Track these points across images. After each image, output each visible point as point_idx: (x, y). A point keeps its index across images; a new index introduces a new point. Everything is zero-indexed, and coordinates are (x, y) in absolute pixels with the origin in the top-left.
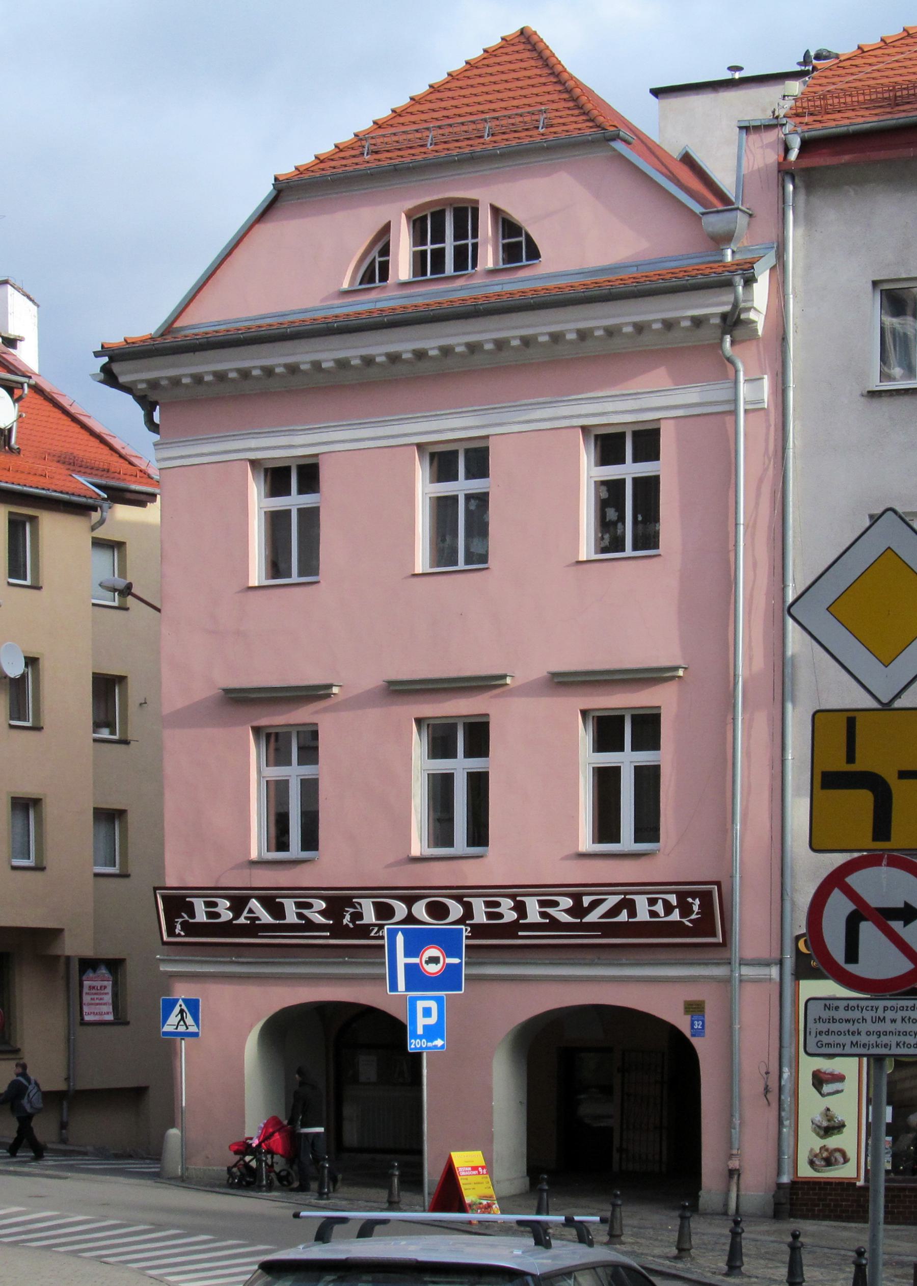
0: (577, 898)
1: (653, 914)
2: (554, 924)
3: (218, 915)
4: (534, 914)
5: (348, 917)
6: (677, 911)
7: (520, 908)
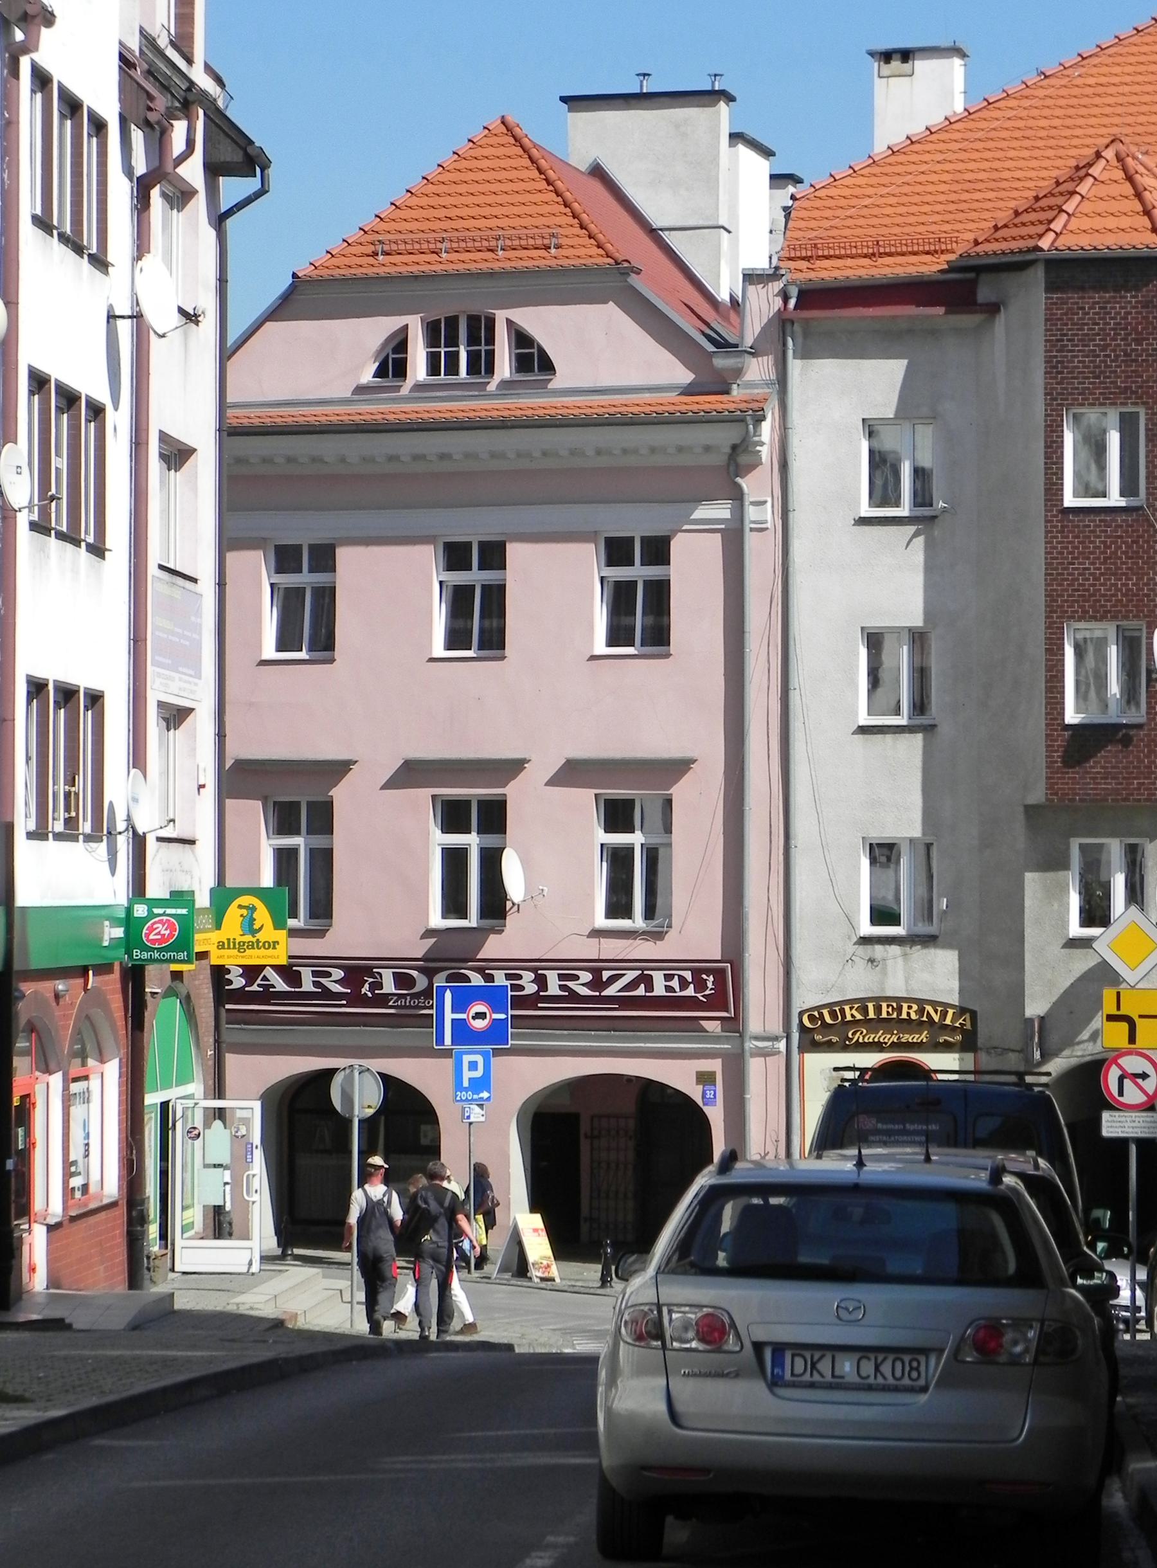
0: (597, 972)
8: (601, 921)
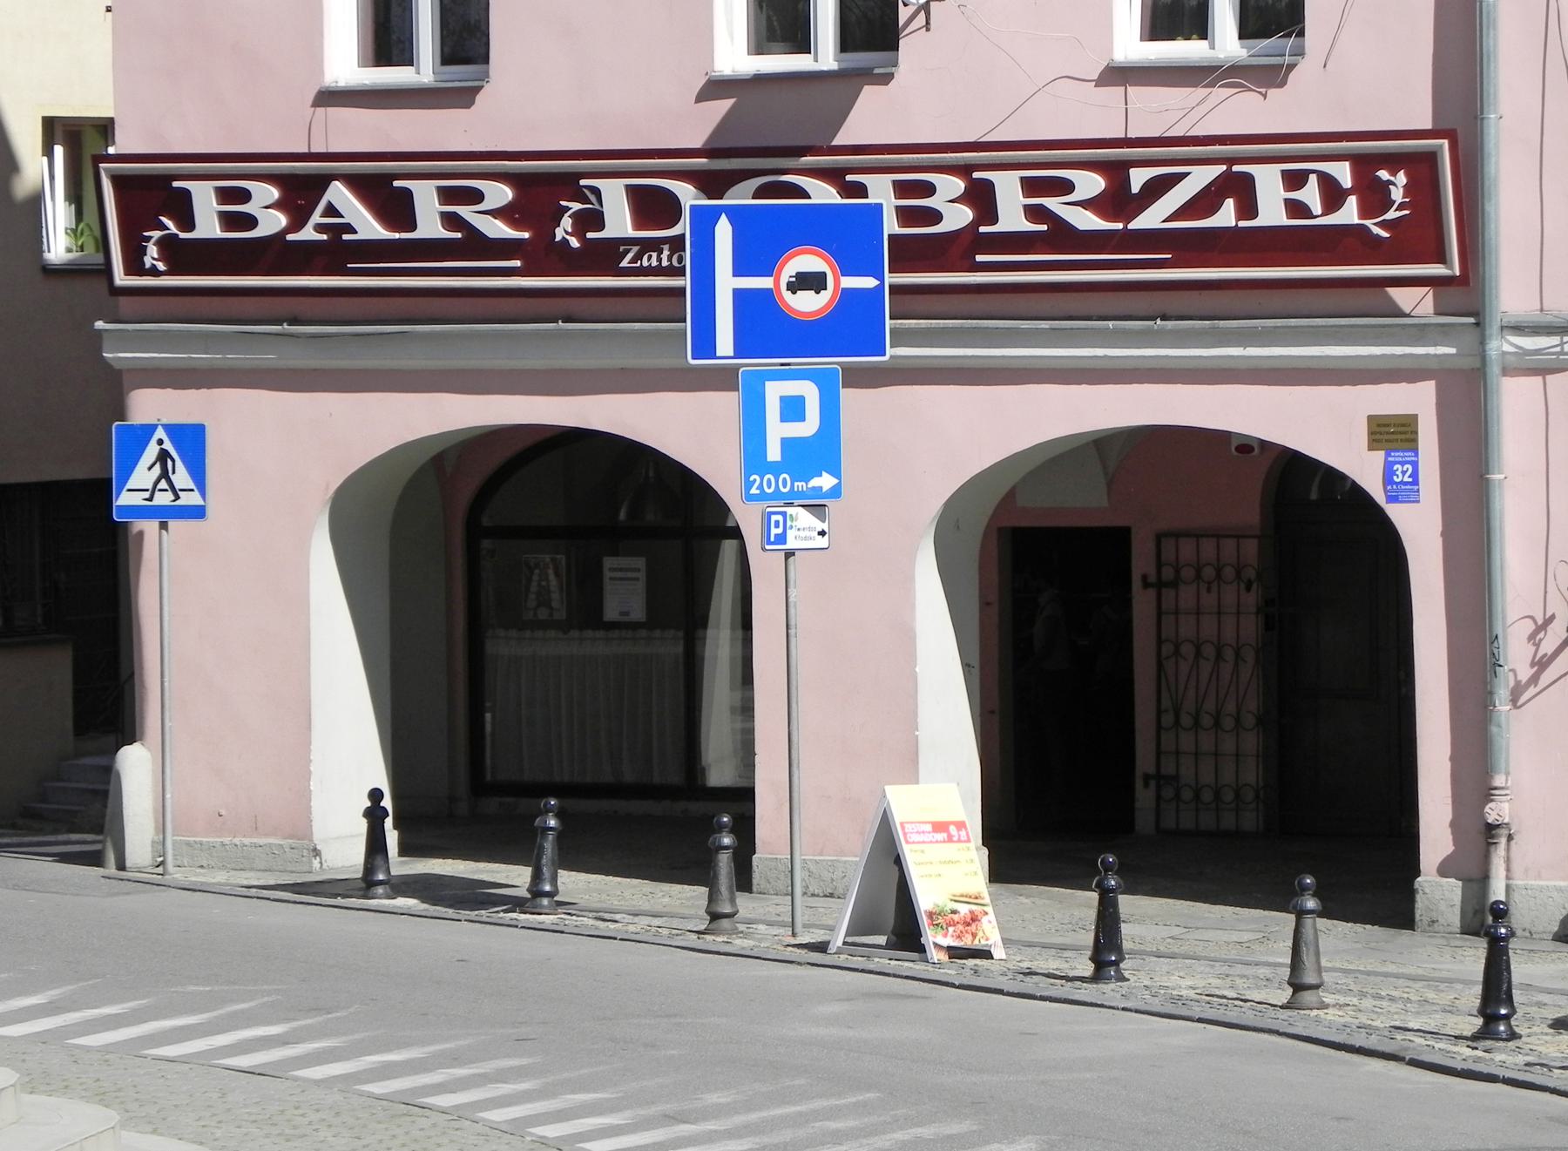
0: (1116, 172)
1: (1296, 208)
2: (1061, 236)
3: (250, 222)
4: (1012, 216)
5: (567, 222)
6: (1352, 201)
7: (982, 198)
8: (1129, 43)
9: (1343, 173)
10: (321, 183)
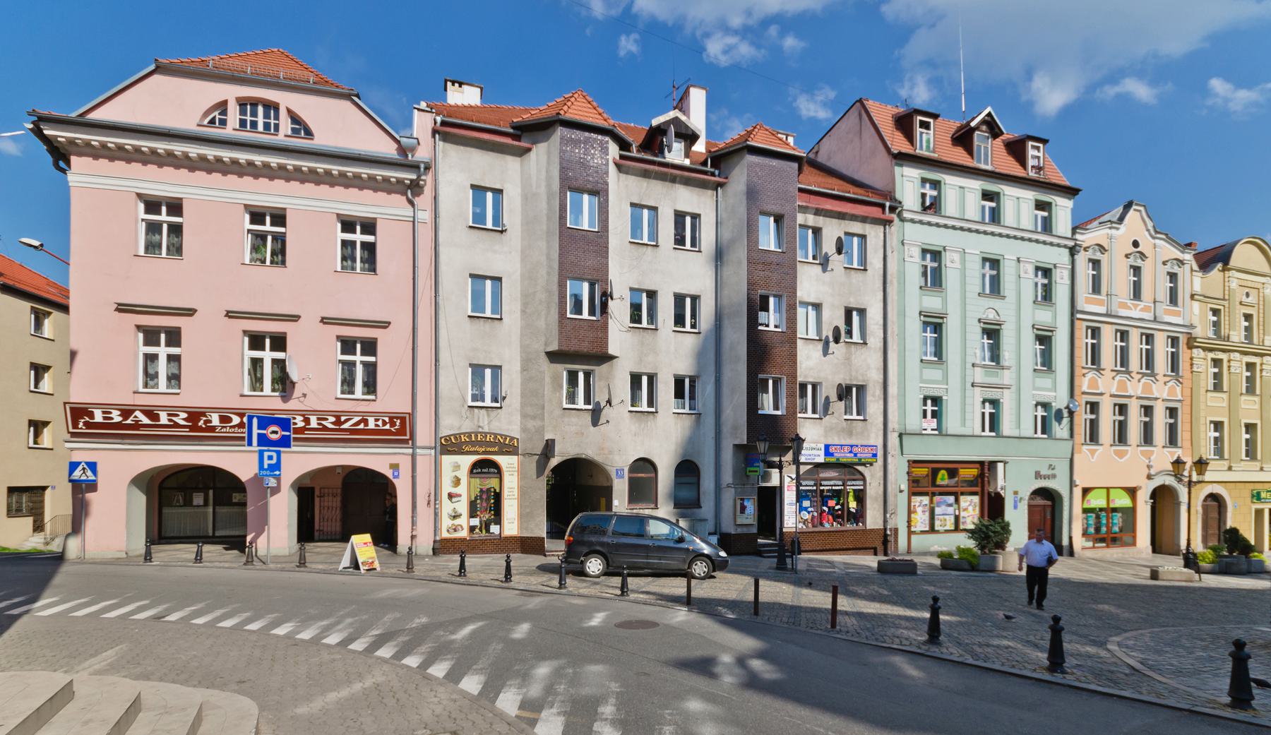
0: (338, 418)
2: (325, 428)
4: (314, 423)
7: (307, 421)
9: (387, 419)
10: (133, 411)
